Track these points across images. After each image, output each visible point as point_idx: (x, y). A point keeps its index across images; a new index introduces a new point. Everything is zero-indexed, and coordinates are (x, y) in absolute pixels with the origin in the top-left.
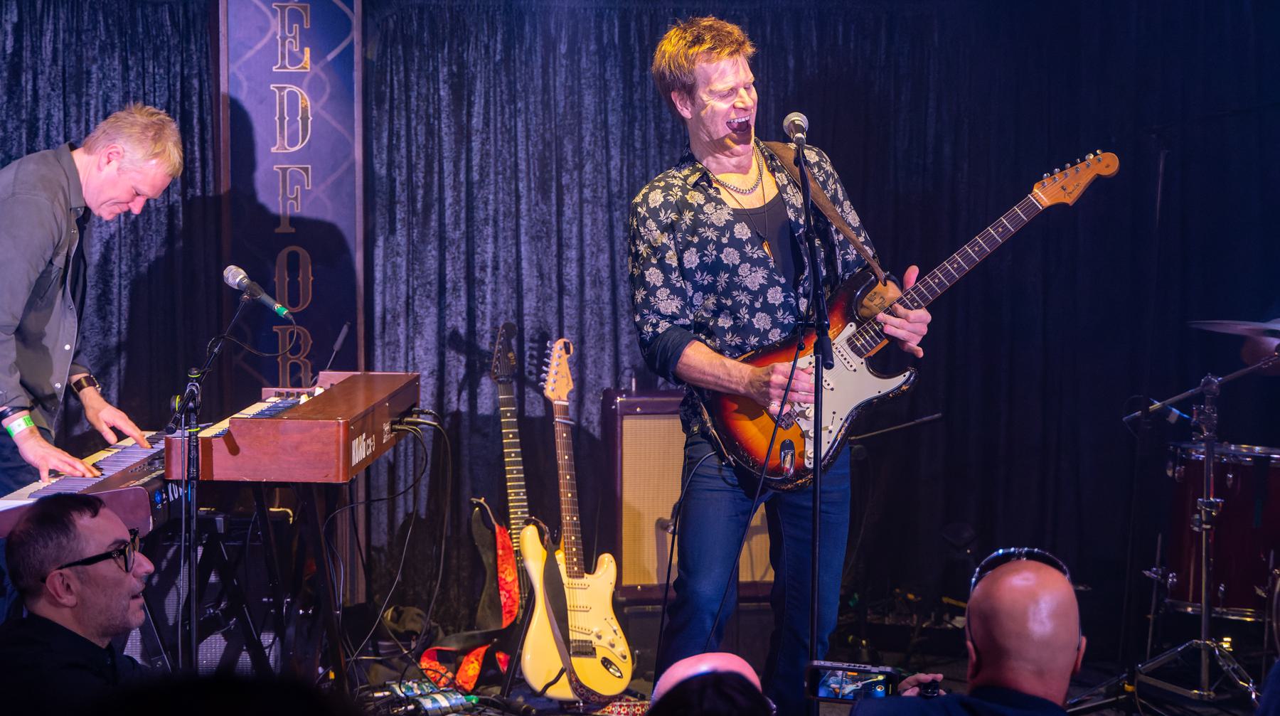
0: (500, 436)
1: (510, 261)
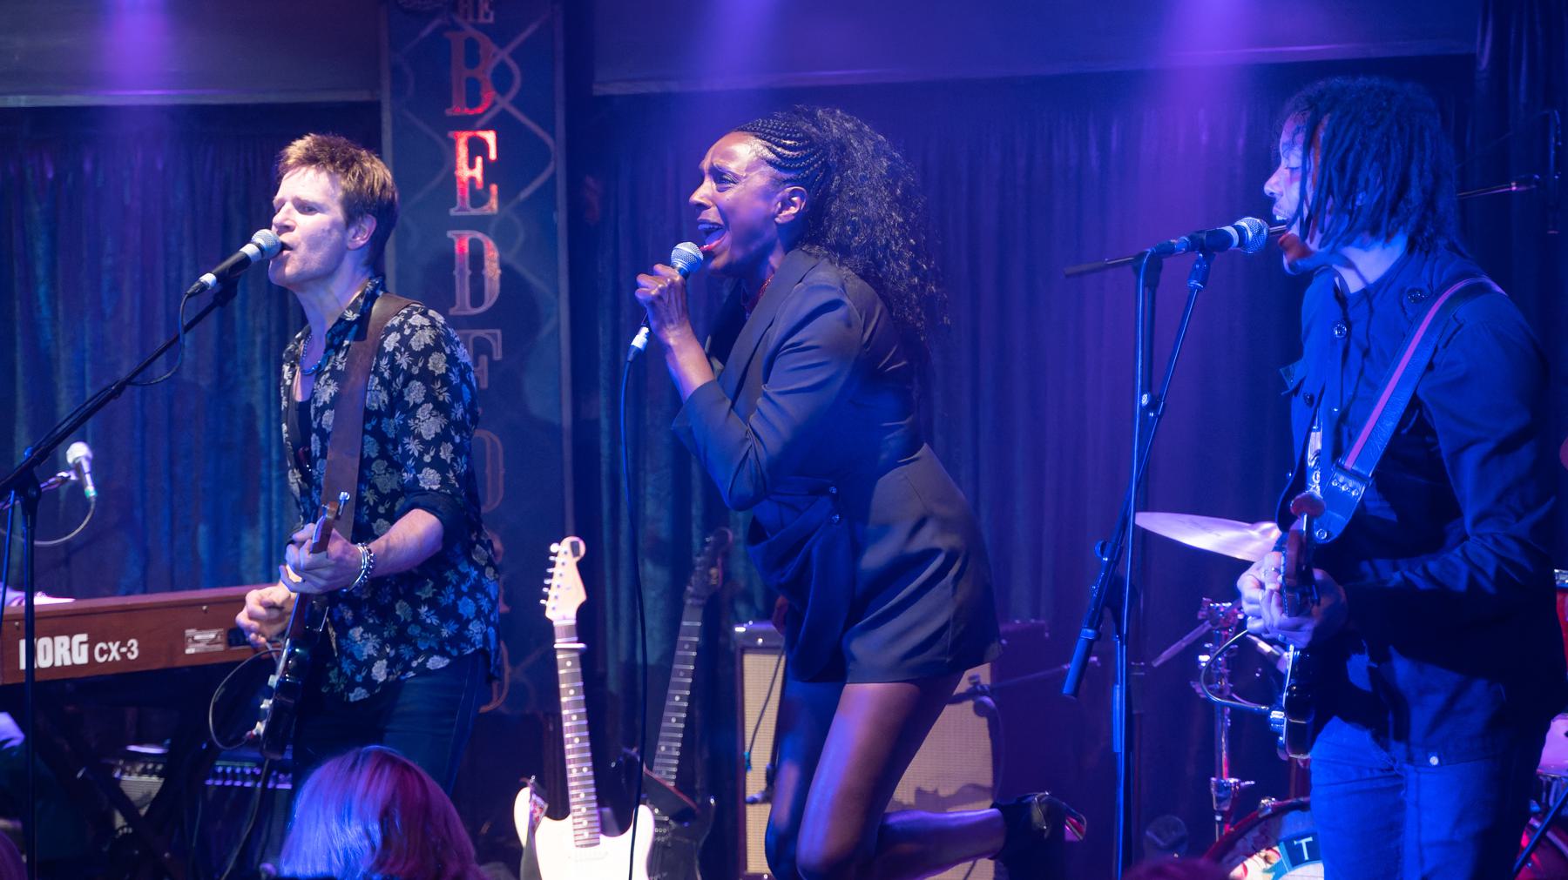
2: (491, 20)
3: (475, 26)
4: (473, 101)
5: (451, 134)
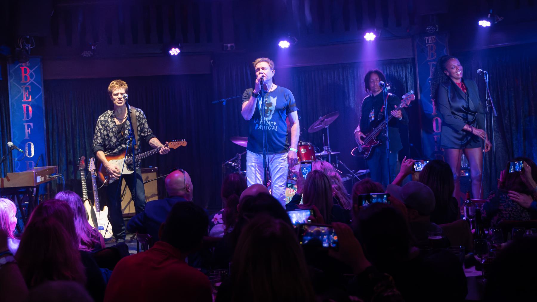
0: (81, 183)
1: (83, 143)
2: (29, 65)
3: (27, 66)
4: (26, 79)
5: (22, 86)
